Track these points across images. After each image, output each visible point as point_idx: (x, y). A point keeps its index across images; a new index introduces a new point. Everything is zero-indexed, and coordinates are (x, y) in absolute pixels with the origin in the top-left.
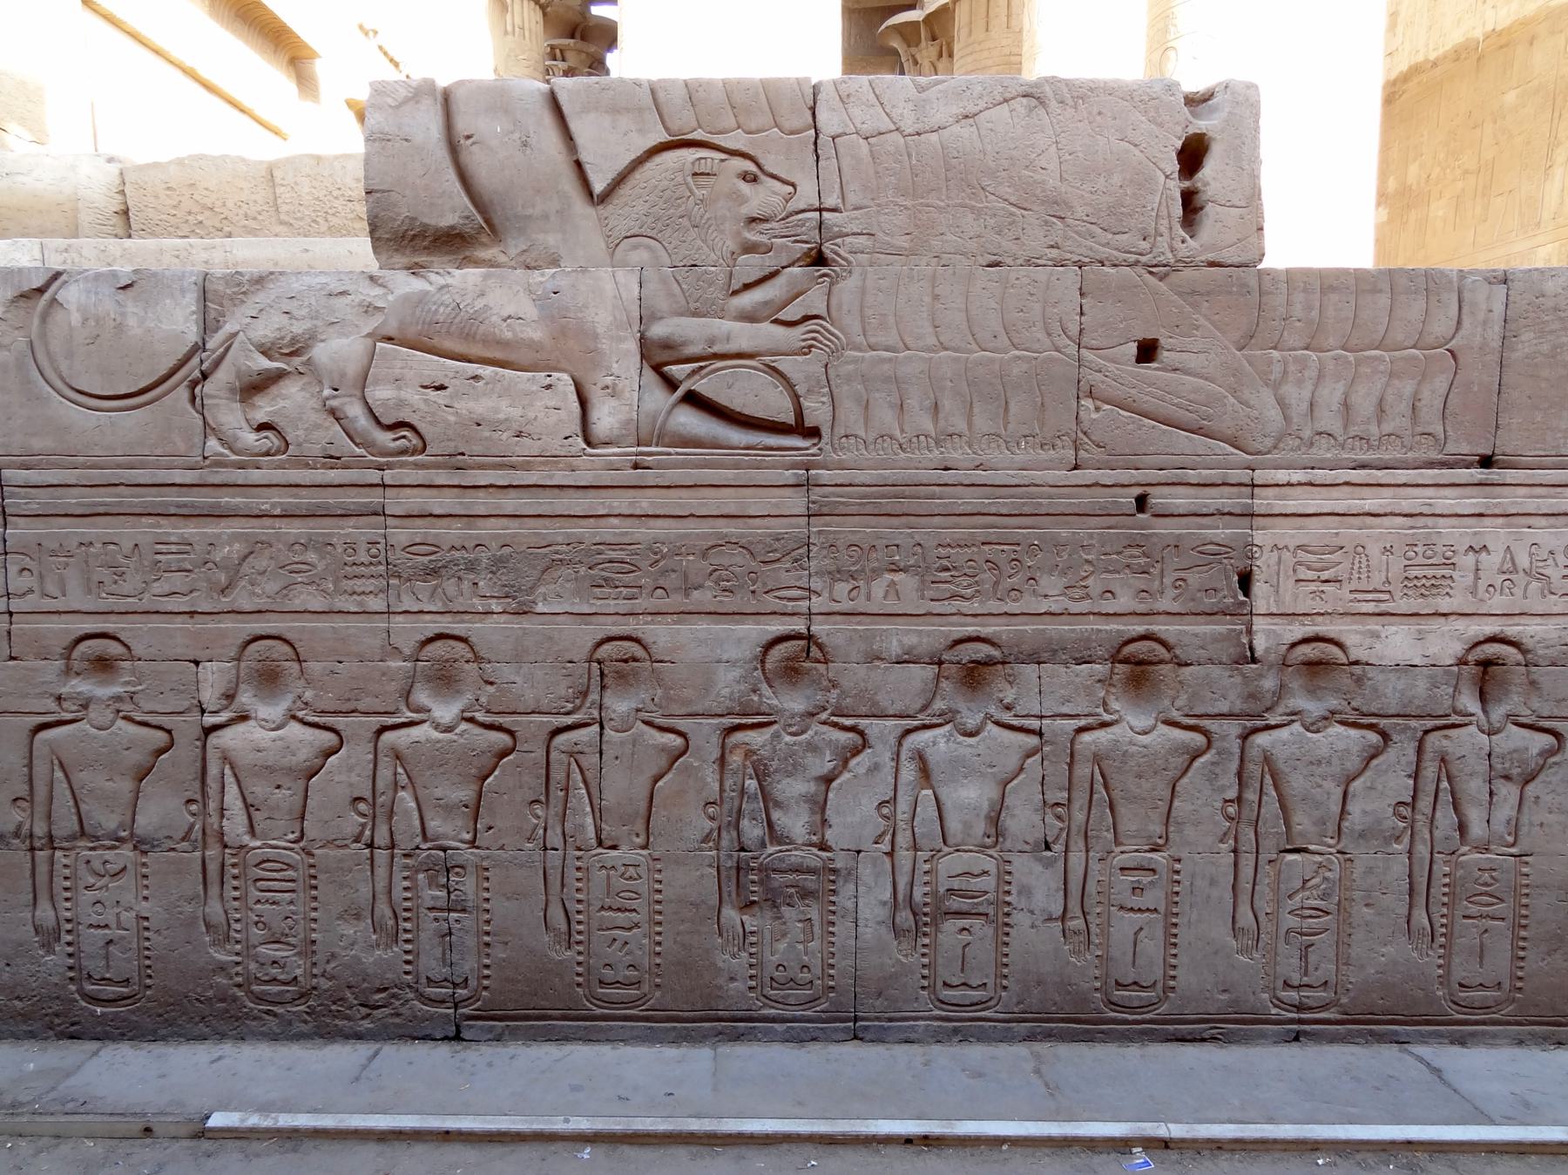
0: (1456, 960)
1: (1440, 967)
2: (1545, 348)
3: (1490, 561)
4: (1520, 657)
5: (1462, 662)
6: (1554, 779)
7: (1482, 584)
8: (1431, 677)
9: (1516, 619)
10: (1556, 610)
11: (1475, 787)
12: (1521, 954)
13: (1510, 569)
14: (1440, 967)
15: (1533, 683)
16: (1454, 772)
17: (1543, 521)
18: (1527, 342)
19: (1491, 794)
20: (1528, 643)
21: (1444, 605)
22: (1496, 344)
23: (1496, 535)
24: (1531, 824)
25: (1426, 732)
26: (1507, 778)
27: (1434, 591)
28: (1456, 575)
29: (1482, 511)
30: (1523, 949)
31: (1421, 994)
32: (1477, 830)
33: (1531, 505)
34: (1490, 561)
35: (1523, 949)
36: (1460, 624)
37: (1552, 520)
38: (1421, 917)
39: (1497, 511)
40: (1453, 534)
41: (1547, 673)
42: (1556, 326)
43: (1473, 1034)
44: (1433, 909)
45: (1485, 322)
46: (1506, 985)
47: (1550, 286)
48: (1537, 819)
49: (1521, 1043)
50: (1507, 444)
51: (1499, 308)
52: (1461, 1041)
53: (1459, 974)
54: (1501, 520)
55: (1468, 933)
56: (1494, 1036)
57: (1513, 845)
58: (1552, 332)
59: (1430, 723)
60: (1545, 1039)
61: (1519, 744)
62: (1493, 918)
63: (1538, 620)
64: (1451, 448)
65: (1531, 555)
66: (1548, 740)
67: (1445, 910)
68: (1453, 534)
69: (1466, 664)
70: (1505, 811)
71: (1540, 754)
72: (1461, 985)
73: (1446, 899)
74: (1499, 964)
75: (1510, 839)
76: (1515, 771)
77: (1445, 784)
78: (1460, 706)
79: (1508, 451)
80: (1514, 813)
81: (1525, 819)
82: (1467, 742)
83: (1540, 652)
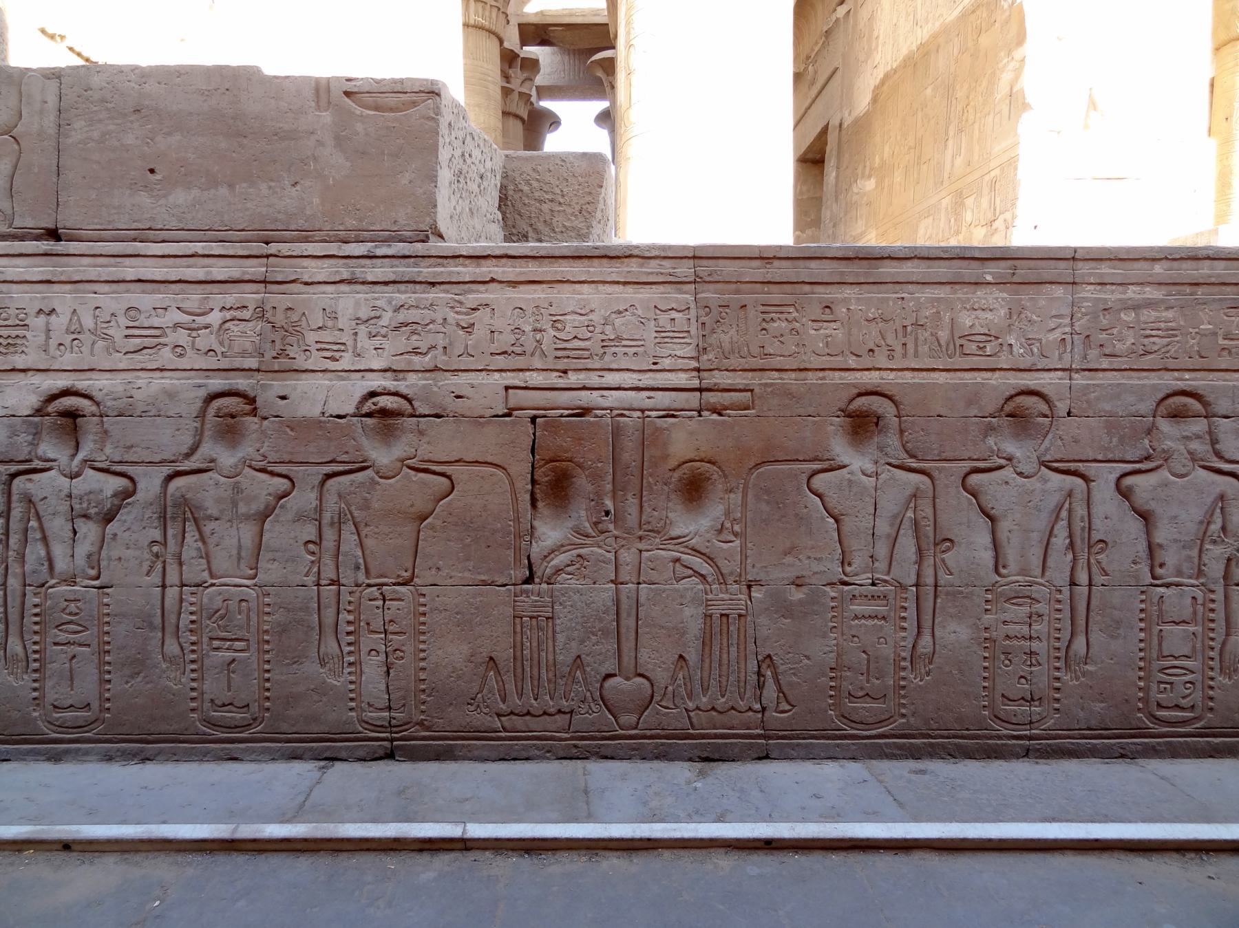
0: (49, 684)
1: (35, 690)
2: (96, 135)
3: (59, 322)
4: (94, 408)
5: (39, 412)
6: (130, 518)
7: (53, 343)
8: (10, 426)
9: (88, 373)
10: (121, 366)
11: (58, 526)
12: (107, 677)
13: (76, 332)
14: (35, 690)
15: (106, 432)
16: (41, 513)
17: (106, 288)
18: (79, 131)
19: (75, 533)
20: (98, 396)
21: (20, 361)
22: (52, 131)
23: (63, 299)
24: (110, 559)
25: (13, 476)
26: (86, 516)
27: (12, 349)
28: (28, 334)
29: (49, 278)
30: (109, 672)
31: (16, 715)
32: (61, 565)
33: (92, 274)
34: (59, 322)
35: (109, 672)
36: (36, 379)
37: (114, 286)
38: (15, 645)
39: (63, 278)
40: (21, 297)
41: (117, 423)
42: (103, 115)
43: (67, 752)
44: (26, 637)
45: (41, 112)
46: (95, 705)
47: (96, 81)
48: (115, 554)
49: (108, 758)
50: (68, 219)
51: (52, 100)
52: (56, 758)
53: (51, 696)
54: (68, 287)
55: (58, 660)
56: (87, 753)
57: (97, 578)
58: (100, 121)
59: (14, 468)
60: (135, 755)
61: (95, 486)
62: (80, 645)
63: (108, 375)
64: (17, 223)
65: (96, 317)
66: (121, 482)
67: (37, 638)
68: (21, 297)
69: (48, 415)
70: (83, 549)
71: (114, 495)
72: (55, 707)
73: (37, 628)
74: (87, 687)
75: (93, 572)
76: (93, 511)
77: (33, 523)
78: (40, 452)
79: (68, 225)
80: (95, 549)
81: (104, 553)
82: (47, 485)
83: (109, 404)
